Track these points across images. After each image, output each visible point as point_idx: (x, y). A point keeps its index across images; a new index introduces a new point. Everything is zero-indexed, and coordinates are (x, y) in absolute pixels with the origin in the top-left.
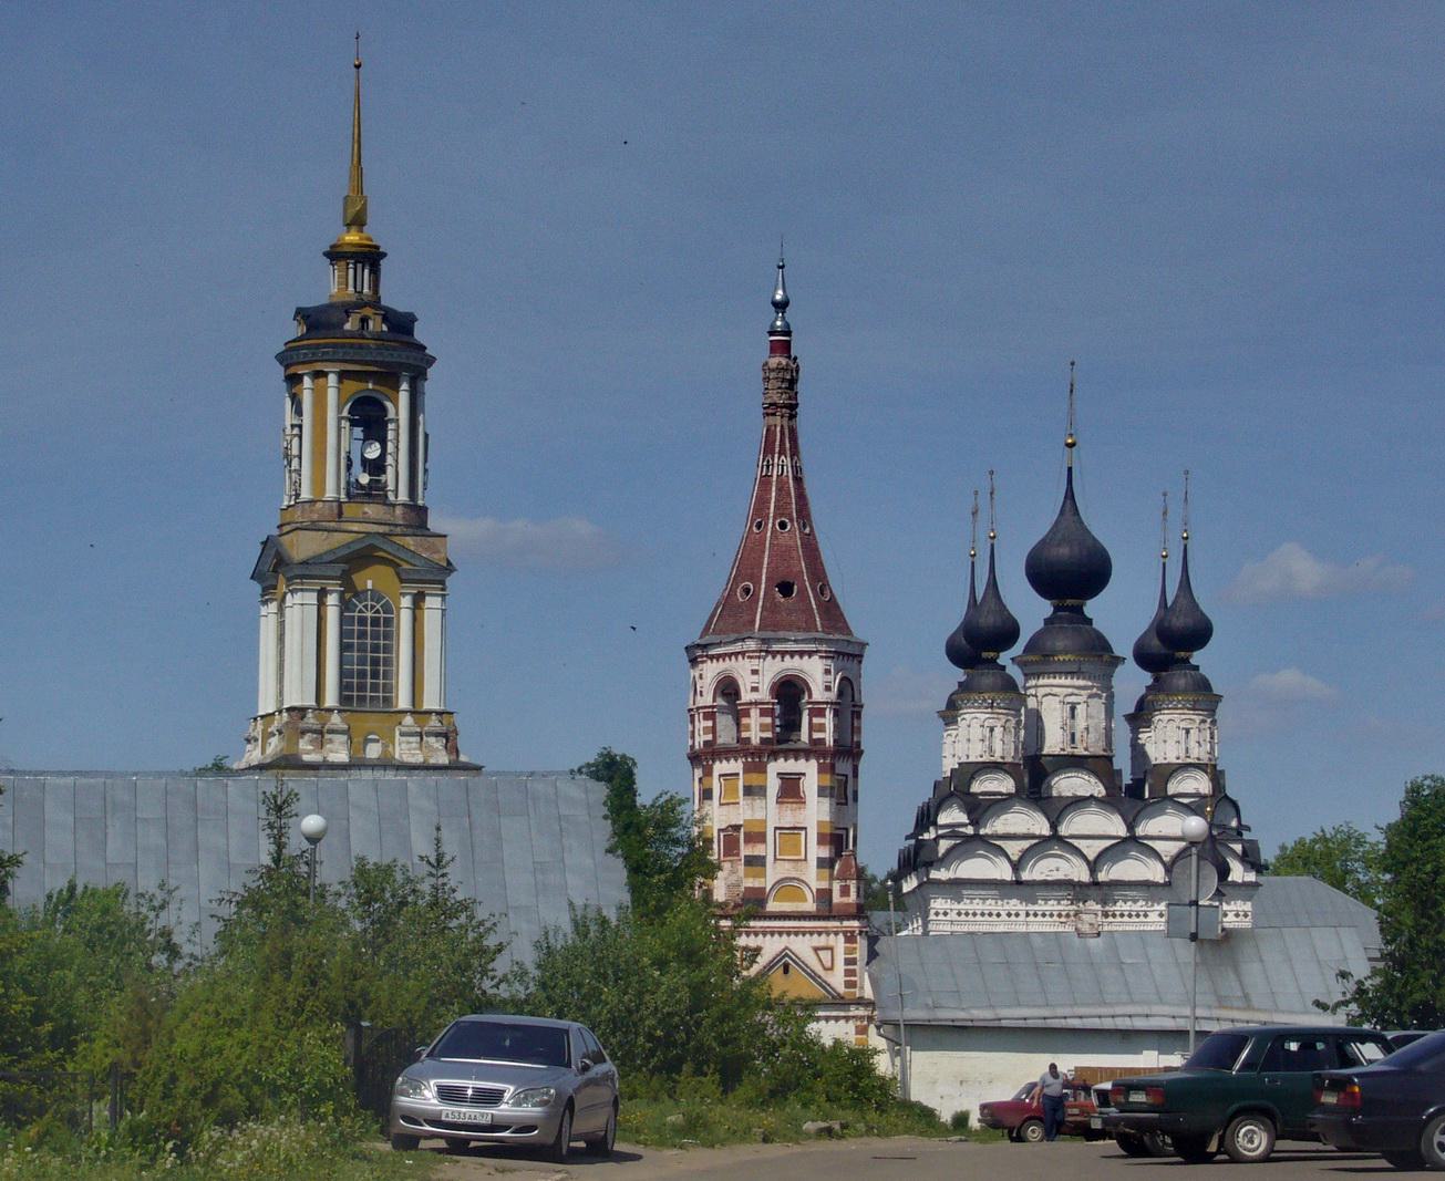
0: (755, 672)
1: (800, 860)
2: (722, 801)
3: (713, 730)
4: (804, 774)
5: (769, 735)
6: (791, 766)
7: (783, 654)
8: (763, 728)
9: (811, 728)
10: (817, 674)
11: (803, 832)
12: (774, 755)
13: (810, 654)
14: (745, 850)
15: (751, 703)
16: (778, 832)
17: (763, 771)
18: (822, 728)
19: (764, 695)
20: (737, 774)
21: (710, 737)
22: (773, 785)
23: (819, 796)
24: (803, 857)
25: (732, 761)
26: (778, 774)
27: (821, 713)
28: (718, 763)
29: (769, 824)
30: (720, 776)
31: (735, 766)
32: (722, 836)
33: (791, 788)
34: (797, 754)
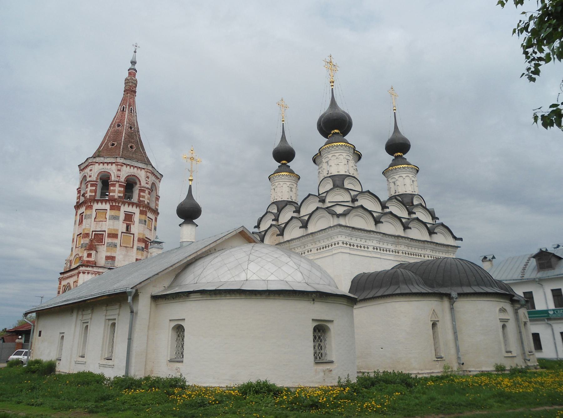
0: (119, 170)
1: (131, 247)
2: (95, 220)
3: (95, 191)
4: (134, 213)
5: (122, 195)
6: (130, 209)
7: (131, 166)
8: (119, 192)
9: (139, 196)
10: (142, 175)
11: (132, 236)
12: (124, 203)
13: (141, 169)
14: (107, 240)
15: (117, 181)
16: (122, 234)
17: (118, 208)
18: (144, 197)
19: (122, 179)
20: (107, 210)
21: (93, 194)
22: (122, 216)
23: (139, 223)
24: (132, 246)
25: (104, 203)
26: (124, 211)
27: (144, 191)
28: (95, 204)
29: (119, 231)
30: (96, 210)
31: (107, 206)
32: (93, 234)
33: (129, 217)
34: (133, 204)
